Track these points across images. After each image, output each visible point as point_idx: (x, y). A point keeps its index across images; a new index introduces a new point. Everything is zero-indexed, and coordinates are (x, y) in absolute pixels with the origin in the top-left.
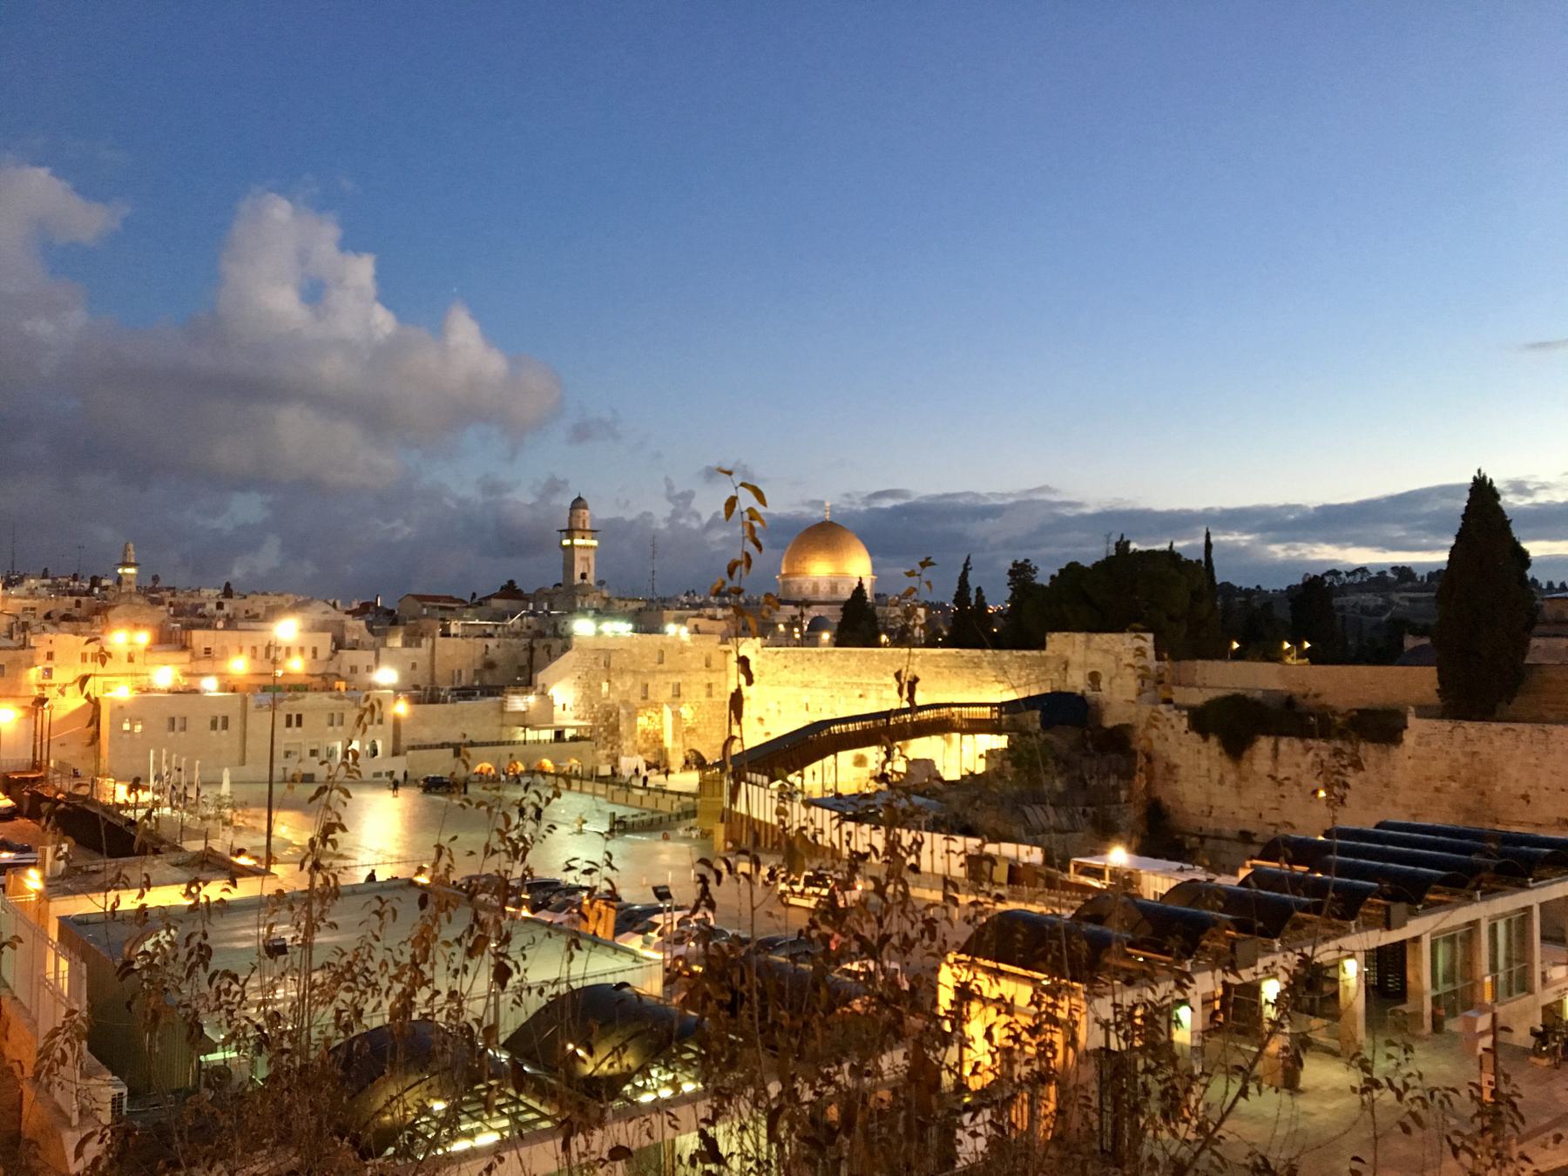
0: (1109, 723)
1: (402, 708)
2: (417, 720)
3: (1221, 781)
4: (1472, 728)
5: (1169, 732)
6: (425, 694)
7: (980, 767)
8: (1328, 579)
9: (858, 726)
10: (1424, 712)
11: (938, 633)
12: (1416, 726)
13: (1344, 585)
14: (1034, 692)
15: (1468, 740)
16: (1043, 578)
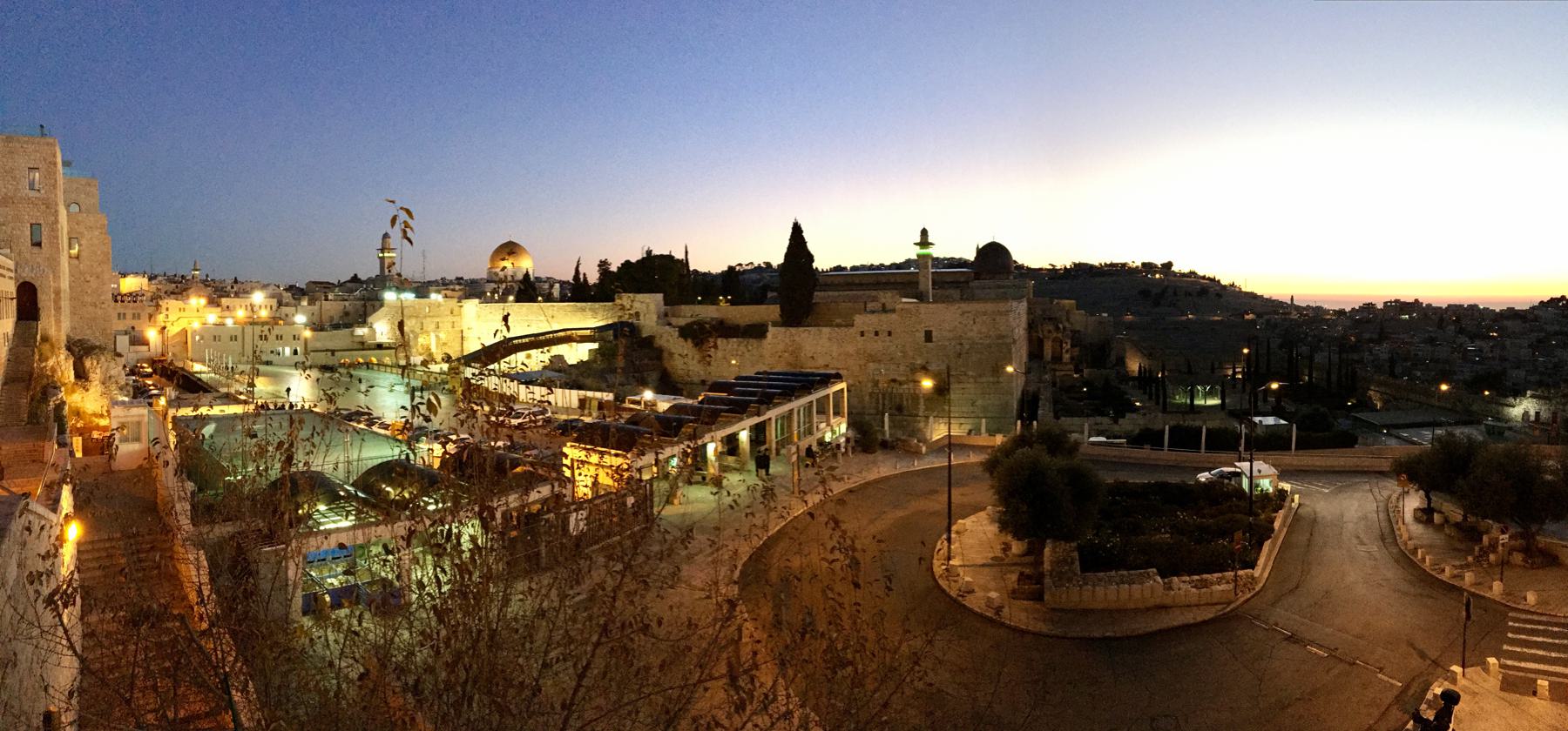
0: (644, 336)
1: (308, 334)
2: (315, 339)
3: (693, 359)
4: (793, 330)
5: (670, 338)
6: (317, 327)
7: (585, 358)
8: (738, 268)
9: (527, 340)
10: (775, 324)
11: (566, 295)
12: (772, 331)
13: (744, 271)
14: (610, 322)
15: (792, 335)
16: (614, 268)
